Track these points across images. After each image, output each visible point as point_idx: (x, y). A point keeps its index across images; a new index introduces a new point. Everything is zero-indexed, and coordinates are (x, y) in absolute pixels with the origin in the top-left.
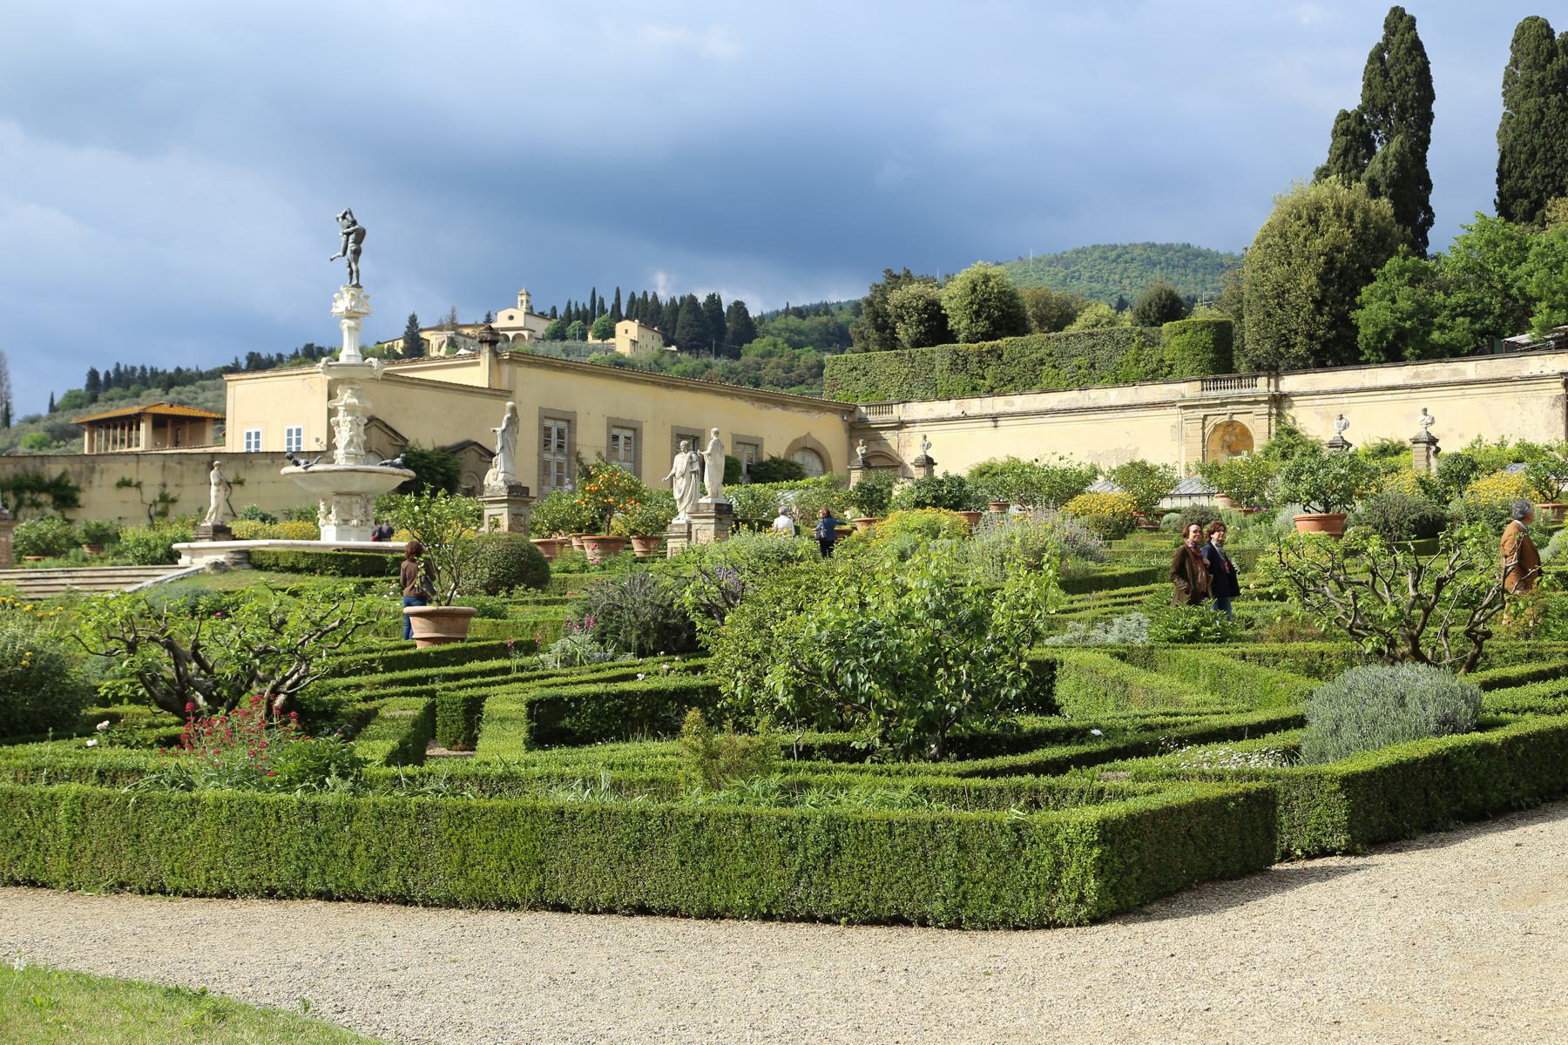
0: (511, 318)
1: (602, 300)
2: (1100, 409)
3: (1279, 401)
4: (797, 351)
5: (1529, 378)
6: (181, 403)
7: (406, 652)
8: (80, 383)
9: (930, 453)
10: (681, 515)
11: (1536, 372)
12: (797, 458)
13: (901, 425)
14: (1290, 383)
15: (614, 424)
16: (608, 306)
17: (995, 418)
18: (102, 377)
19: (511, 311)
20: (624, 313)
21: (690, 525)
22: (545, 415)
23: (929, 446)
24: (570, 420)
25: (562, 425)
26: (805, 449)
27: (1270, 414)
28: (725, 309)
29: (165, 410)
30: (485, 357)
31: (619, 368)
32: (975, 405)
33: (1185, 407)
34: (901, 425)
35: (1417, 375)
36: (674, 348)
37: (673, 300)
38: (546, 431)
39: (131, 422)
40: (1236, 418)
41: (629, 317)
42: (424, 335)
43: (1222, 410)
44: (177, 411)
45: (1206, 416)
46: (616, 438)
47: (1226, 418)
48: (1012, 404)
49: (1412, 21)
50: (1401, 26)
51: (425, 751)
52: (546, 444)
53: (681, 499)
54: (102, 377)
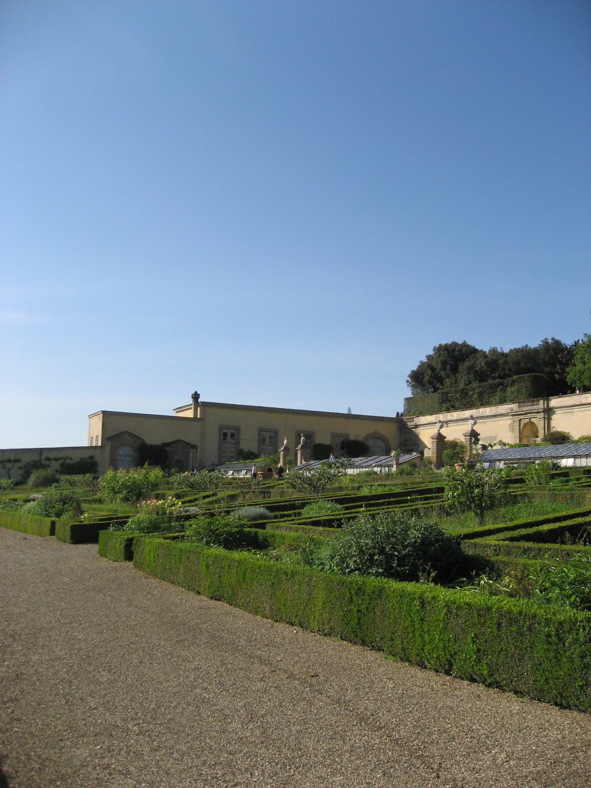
3: (549, 412)
13: (416, 426)
14: (555, 402)
26: (375, 438)
27: (544, 418)
33: (512, 415)
34: (416, 426)
40: (532, 420)
43: (526, 416)
47: (527, 420)
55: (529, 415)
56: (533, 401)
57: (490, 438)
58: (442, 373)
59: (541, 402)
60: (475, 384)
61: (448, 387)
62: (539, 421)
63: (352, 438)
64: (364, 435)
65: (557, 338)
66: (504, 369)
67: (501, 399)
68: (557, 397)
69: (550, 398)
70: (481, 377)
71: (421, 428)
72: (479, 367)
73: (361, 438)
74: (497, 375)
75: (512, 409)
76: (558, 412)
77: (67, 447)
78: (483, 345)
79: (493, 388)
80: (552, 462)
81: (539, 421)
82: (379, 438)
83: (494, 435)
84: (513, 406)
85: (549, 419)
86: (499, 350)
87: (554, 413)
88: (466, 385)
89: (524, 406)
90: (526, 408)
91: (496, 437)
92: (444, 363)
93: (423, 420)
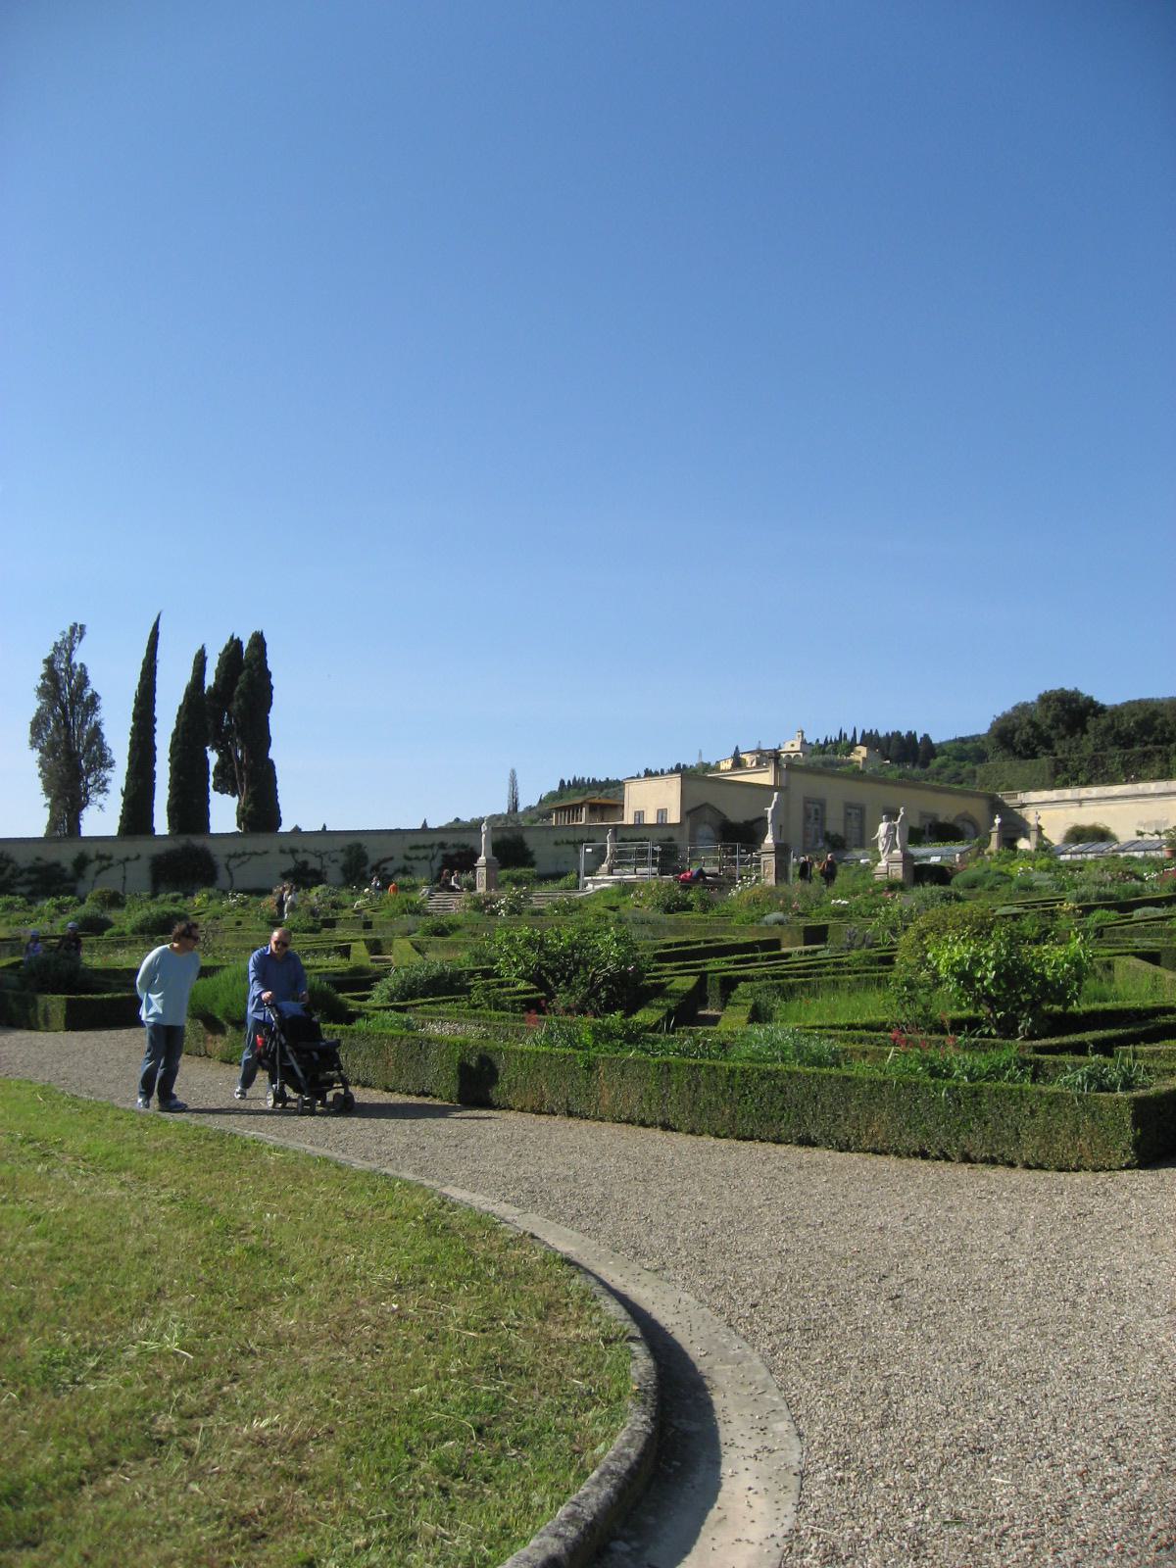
0: (793, 745)
1: (845, 735)
2: (1145, 796)
4: (962, 764)
6: (608, 798)
7: (713, 945)
8: (556, 788)
9: (1040, 822)
10: (883, 861)
12: (959, 825)
13: (1023, 806)
15: (848, 806)
16: (849, 737)
17: (1080, 801)
18: (566, 784)
19: (792, 742)
20: (858, 741)
21: (888, 866)
22: (807, 801)
23: (1039, 818)
24: (822, 804)
25: (818, 807)
26: (964, 820)
28: (919, 740)
29: (596, 801)
30: (771, 768)
31: (857, 774)
32: (1068, 793)
34: (1023, 806)
36: (888, 762)
37: (887, 734)
38: (806, 810)
39: (577, 808)
41: (861, 744)
42: (743, 756)
44: (604, 801)
46: (850, 814)
48: (1091, 793)
51: (696, 1011)
52: (807, 817)
53: (883, 851)
54: (566, 784)
57: (1157, 822)
58: (1053, 733)
60: (1114, 751)
61: (1064, 752)
63: (941, 820)
64: (954, 816)
66: (1163, 732)
67: (1162, 771)
70: (1125, 741)
71: (1032, 808)
72: (1126, 725)
73: (950, 820)
74: (1151, 739)
77: (222, 834)
78: (1110, 693)
79: (1147, 755)
82: (969, 821)
83: (1165, 819)
88: (1096, 750)
91: (1167, 822)
92: (1057, 719)
93: (1034, 796)
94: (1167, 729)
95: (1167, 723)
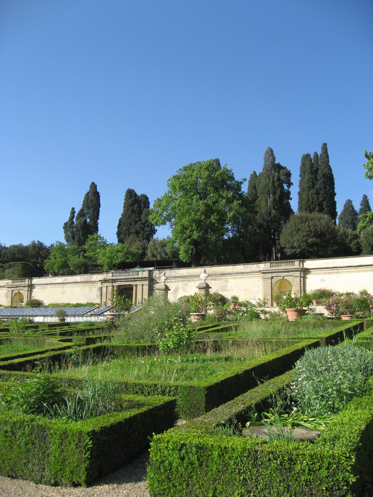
3: (31, 287)
5: (92, 282)
11: (95, 280)
14: (35, 281)
27: (28, 290)
35: (65, 280)
40: (20, 291)
45: (13, 291)
47: (17, 291)
49: (96, 186)
50: (93, 187)
55: (19, 288)
56: (22, 279)
59: (27, 280)
62: (24, 292)
65: (41, 241)
66: (4, 257)
68: (37, 278)
69: (33, 278)
75: (8, 283)
76: (37, 287)
80: (29, 319)
81: (24, 292)
84: (9, 281)
85: (31, 291)
86: (3, 245)
87: (34, 288)
89: (16, 282)
90: (17, 284)
94: (6, 256)
95: (6, 253)
